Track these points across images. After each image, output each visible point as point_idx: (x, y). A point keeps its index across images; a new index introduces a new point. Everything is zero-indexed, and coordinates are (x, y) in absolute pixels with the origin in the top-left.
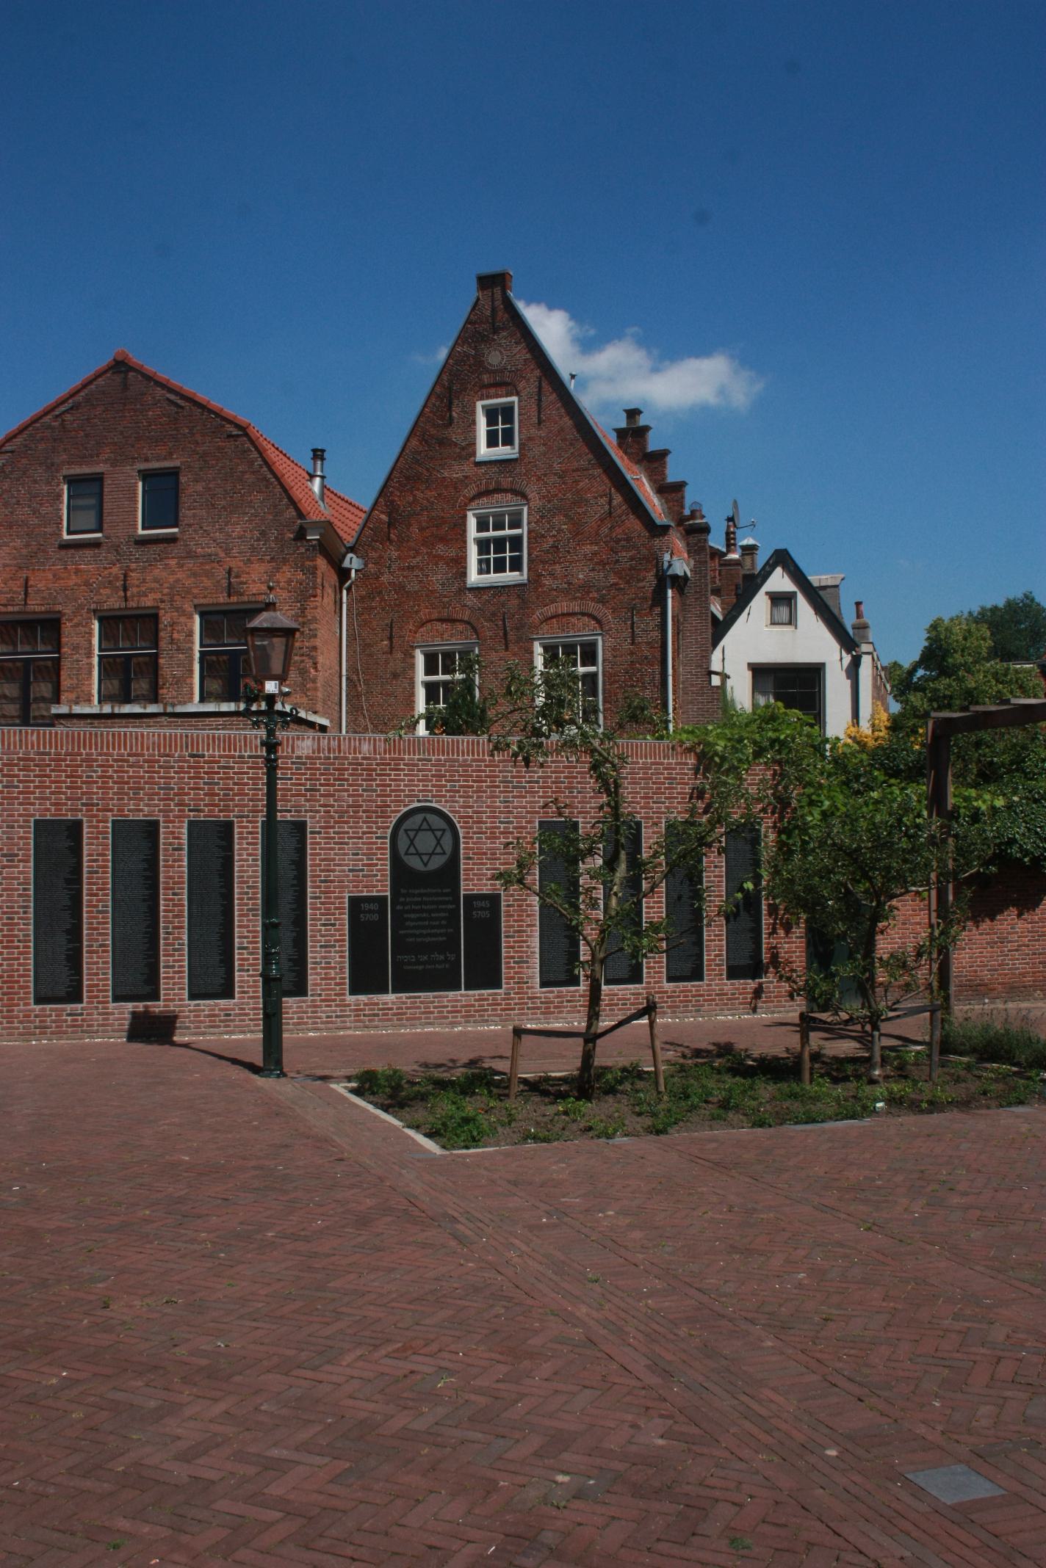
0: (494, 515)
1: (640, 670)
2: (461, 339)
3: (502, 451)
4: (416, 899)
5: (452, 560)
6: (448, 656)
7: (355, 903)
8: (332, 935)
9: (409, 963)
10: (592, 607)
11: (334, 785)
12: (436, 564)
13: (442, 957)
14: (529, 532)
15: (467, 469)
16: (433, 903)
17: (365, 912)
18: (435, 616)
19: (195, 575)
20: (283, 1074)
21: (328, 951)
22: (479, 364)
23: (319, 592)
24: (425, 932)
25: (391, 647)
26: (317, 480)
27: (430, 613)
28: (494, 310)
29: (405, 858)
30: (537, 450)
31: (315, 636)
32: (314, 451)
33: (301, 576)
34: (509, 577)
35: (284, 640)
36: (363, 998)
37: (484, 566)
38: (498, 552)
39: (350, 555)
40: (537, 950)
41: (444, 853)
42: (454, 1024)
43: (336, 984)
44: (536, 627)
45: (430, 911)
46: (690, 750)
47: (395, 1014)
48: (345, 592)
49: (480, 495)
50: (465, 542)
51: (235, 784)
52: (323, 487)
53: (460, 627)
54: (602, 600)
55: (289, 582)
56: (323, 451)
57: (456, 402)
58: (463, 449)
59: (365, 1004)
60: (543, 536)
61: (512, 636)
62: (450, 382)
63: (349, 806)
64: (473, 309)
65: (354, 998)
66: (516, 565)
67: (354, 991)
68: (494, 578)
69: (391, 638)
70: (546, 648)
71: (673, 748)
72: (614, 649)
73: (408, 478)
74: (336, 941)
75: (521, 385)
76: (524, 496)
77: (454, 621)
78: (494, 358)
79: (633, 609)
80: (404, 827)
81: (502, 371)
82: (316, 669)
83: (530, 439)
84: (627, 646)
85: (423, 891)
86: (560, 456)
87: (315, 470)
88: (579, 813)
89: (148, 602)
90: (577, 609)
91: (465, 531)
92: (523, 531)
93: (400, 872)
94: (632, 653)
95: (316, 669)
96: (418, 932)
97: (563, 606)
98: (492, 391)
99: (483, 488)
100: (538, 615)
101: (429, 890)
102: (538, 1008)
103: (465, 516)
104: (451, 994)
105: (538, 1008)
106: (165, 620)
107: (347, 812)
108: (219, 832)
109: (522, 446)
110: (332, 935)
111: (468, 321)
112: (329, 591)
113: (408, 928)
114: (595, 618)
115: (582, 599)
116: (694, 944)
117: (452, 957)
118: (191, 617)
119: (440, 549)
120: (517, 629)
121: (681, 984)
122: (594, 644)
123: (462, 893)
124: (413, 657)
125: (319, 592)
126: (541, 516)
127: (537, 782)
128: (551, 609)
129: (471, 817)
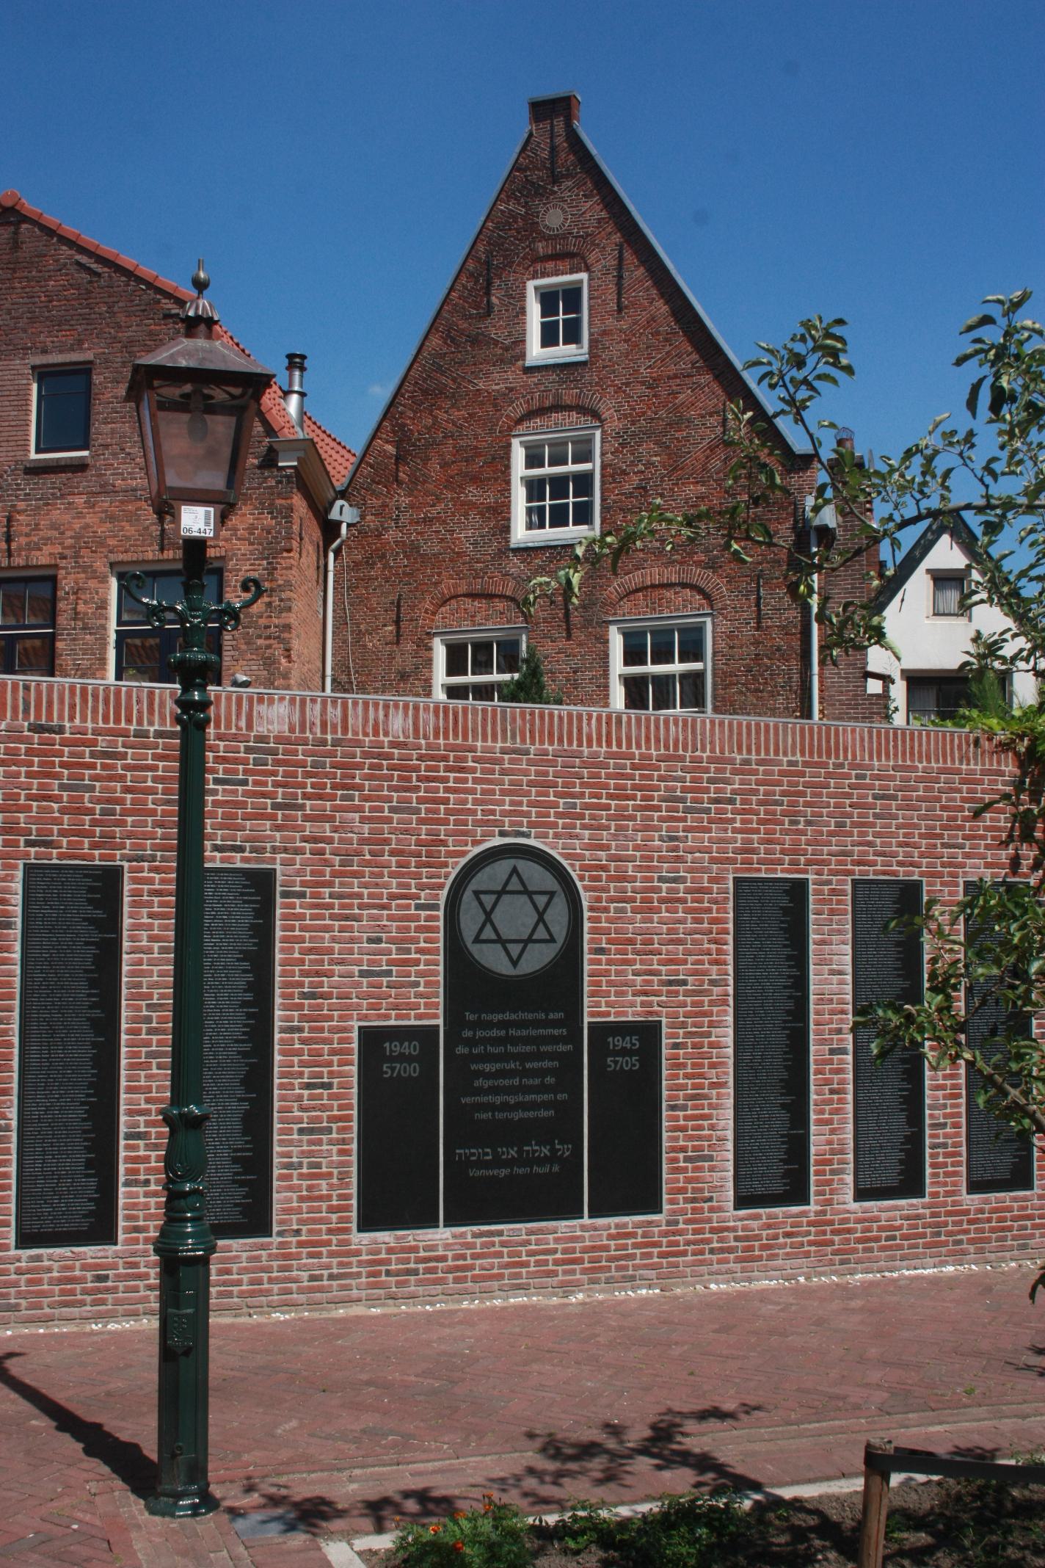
0: (552, 444)
1: (768, 668)
2: (506, 193)
3: (564, 352)
4: (495, 1033)
5: (489, 508)
6: (482, 648)
7: (372, 1039)
8: (323, 1108)
11: (333, 798)
12: (466, 515)
13: (546, 1151)
14: (603, 467)
15: (513, 376)
17: (392, 1059)
18: (463, 589)
19: (112, 518)
20: (208, 1503)
21: (315, 1144)
22: (531, 229)
23: (295, 544)
24: (512, 1100)
25: (398, 635)
26: (294, 399)
27: (455, 586)
28: (553, 150)
29: (475, 949)
30: (616, 349)
32: (291, 357)
33: (268, 521)
34: (571, 532)
35: (232, 420)
36: (386, 1237)
37: (535, 518)
38: (556, 499)
39: (339, 503)
40: (730, 1134)
41: (552, 940)
42: (567, 1287)
43: (332, 1210)
44: (613, 605)
45: (523, 1058)
46: (1005, 747)
47: (450, 1270)
48: (331, 556)
49: (530, 415)
50: (508, 483)
51: (127, 790)
52: (302, 412)
53: (500, 605)
54: (712, 565)
55: (251, 529)
56: (303, 357)
58: (506, 349)
60: (624, 473)
61: (576, 618)
62: (489, 253)
63: (362, 841)
64: (524, 149)
65: (367, 1237)
66: (583, 516)
67: (366, 1224)
68: (550, 534)
69: (397, 622)
70: (627, 635)
71: (977, 742)
72: (730, 636)
73: (425, 392)
74: (332, 1119)
75: (591, 258)
76: (596, 415)
77: (490, 596)
78: (554, 219)
79: (759, 577)
80: (474, 885)
81: (564, 237)
82: (289, 657)
83: (604, 333)
84: (749, 632)
85: (508, 1016)
87: (291, 384)
88: (809, 863)
89: (41, 558)
90: (674, 579)
91: (508, 467)
92: (595, 466)
93: (465, 979)
94: (757, 643)
95: (289, 657)
96: (498, 1100)
97: (655, 574)
99: (535, 404)
101: (522, 1016)
102: (730, 1250)
103: (508, 446)
104: (563, 1225)
105: (730, 1250)
106: (66, 584)
107: (359, 853)
108: (91, 890)
109: (593, 343)
110: (323, 1108)
111: (516, 167)
113: (480, 1092)
114: (700, 591)
115: (681, 563)
117: (565, 1150)
118: (104, 580)
119: (472, 493)
121: (992, 1196)
122: (700, 629)
123: (586, 1020)
124: (431, 649)
125: (295, 544)
126: (622, 442)
127: (731, 801)
128: (636, 579)
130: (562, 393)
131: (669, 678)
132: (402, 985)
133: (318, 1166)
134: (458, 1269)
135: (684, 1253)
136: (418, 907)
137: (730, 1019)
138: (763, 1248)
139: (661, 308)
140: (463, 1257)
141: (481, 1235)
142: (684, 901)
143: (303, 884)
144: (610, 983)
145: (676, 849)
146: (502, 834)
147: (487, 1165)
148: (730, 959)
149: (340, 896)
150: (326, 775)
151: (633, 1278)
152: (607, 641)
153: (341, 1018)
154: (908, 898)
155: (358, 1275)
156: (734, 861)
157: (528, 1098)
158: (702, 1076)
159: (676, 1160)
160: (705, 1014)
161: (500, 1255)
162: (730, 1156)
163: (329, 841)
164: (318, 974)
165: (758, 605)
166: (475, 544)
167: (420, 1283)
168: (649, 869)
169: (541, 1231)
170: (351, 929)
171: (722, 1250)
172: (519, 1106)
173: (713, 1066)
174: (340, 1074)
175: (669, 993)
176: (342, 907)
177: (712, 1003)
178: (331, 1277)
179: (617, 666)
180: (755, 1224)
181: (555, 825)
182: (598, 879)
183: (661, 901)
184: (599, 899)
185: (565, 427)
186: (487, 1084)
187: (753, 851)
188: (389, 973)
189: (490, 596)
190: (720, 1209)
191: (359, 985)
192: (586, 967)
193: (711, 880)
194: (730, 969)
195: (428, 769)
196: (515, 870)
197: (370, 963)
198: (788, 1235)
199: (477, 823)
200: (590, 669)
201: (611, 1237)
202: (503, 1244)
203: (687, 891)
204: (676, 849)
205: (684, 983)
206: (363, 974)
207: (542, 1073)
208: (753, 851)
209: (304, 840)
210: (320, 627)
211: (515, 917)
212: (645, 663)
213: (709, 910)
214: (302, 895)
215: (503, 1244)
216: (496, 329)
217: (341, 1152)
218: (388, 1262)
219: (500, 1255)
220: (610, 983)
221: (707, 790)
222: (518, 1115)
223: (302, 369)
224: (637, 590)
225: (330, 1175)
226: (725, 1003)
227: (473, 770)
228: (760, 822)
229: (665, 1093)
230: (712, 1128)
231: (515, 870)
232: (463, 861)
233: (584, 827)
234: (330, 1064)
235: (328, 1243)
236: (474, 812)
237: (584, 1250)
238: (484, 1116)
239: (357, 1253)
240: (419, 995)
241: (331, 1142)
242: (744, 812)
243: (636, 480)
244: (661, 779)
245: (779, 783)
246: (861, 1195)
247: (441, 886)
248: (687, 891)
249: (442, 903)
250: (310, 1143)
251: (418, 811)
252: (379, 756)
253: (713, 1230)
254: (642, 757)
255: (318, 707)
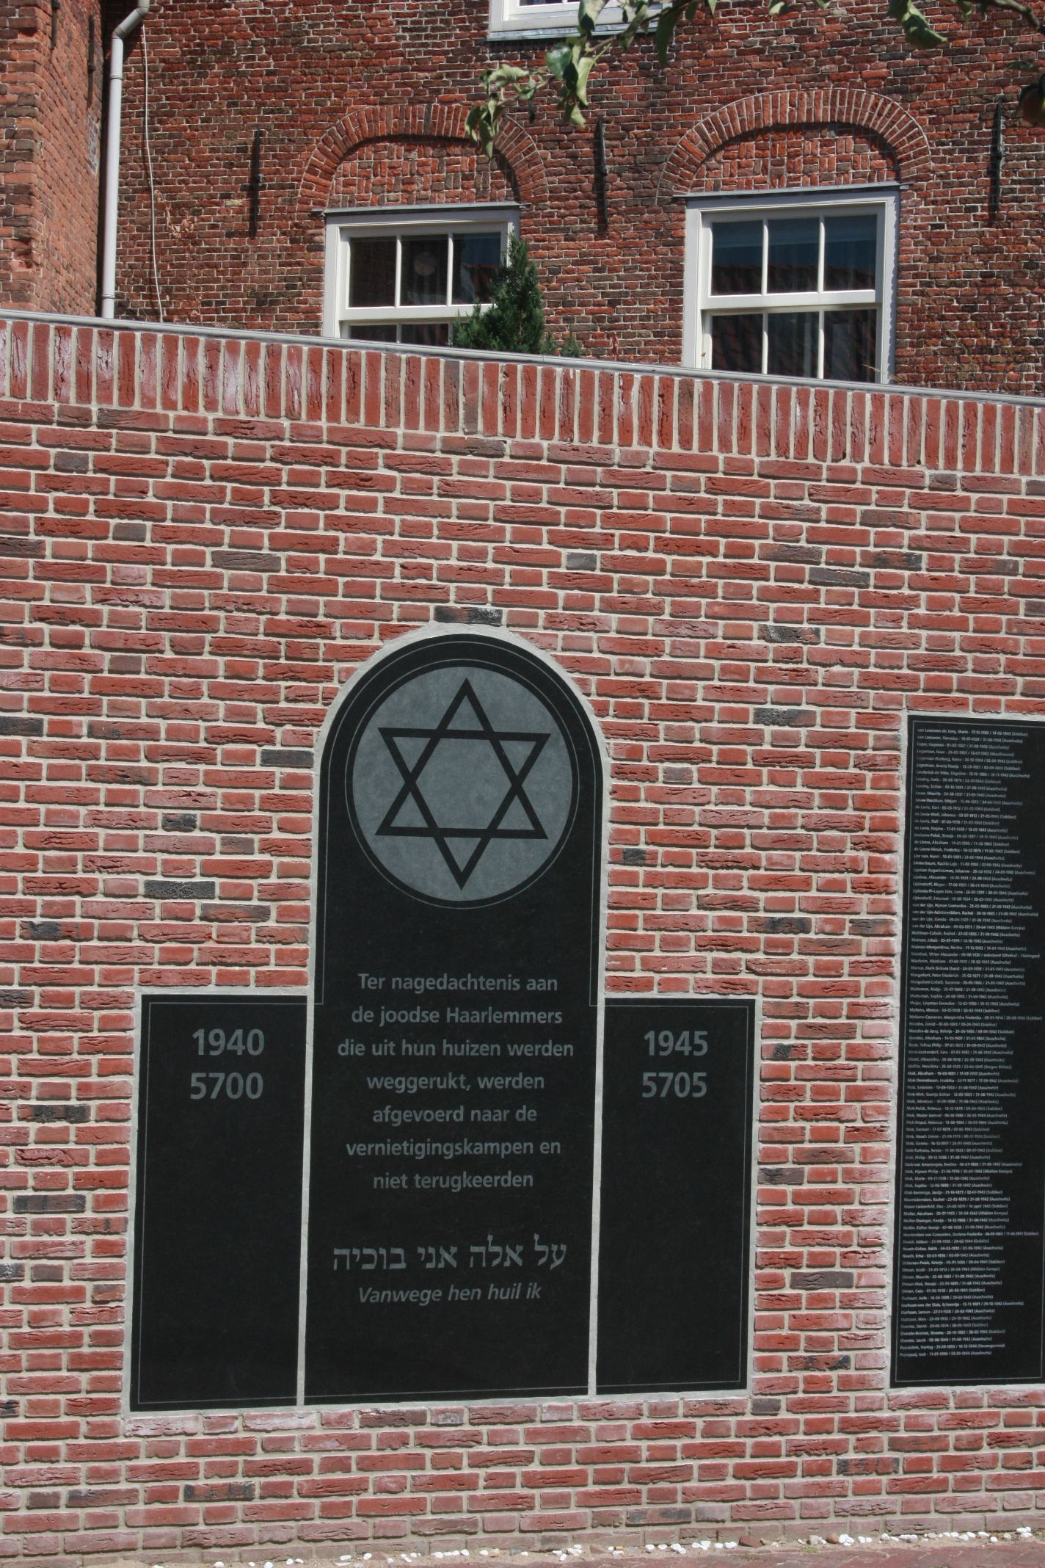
1: (1008, 303)
4: (417, 1016)
6: (425, 248)
7: (171, 1024)
8: (67, 1159)
9: (383, 1279)
10: (868, 106)
11: (98, 532)
13: (514, 1256)
16: (483, 1033)
17: (209, 1064)
18: (389, 124)
23: (42, 18)
24: (449, 1151)
25: (254, 217)
27: (373, 117)
29: (382, 847)
31: (29, 155)
36: (187, 1421)
40: (887, 1233)
41: (538, 833)
43: (79, 1364)
44: (694, 165)
48: (118, 46)
54: (903, 87)
59: (196, 1449)
61: (618, 190)
63: (159, 623)
69: (252, 190)
70: (720, 230)
72: (934, 235)
74: (86, 1182)
80: (383, 717)
84: (972, 228)
90: (823, 113)
94: (987, 250)
95: (27, 254)
96: (421, 1150)
97: (782, 101)
100: (695, 135)
101: (474, 982)
102: (882, 1467)
105: (882, 1467)
107: (151, 647)
110: (67, 1159)
112: (73, 28)
114: (876, 140)
115: (838, 81)
117: (553, 1255)
120: (636, 169)
122: (871, 220)
123: (603, 994)
124: (320, 248)
125: (42, 18)
127: (910, 562)
128: (744, 111)
129: (647, 691)
131: (805, 319)
132: (231, 916)
133: (55, 1275)
134: (331, 1488)
135: (788, 1471)
136: (269, 759)
137: (893, 1002)
138: (948, 1464)
140: (343, 1465)
141: (380, 1421)
142: (806, 761)
143: (36, 705)
144: (653, 923)
145: (794, 656)
146: (443, 616)
147: (397, 1281)
148: (897, 881)
149: (112, 733)
150: (88, 486)
151: (683, 1517)
152: (680, 241)
153: (108, 979)
155: (131, 1496)
156: (911, 684)
157: (481, 1148)
158: (832, 1114)
159: (776, 1282)
160: (842, 991)
161: (417, 1462)
162: (887, 1277)
163: (91, 620)
164: (62, 888)
165: (993, 172)
166: (415, 29)
167: (254, 1516)
168: (739, 695)
169: (501, 1417)
170: (132, 801)
171: (864, 1467)
172: (463, 1163)
173: (856, 1095)
174: (104, 1093)
175: (771, 947)
176: (115, 754)
177: (857, 969)
178: (75, 1500)
179: (700, 292)
180: (932, 1416)
181: (550, 601)
182: (635, 712)
184: (635, 754)
186: (400, 1118)
187: (953, 665)
188: (207, 891)
189: (444, 142)
190: (862, 1384)
191: (145, 912)
192: (606, 890)
193: (864, 722)
194: (897, 901)
195: (296, 479)
196: (466, 690)
197: (169, 868)
198: (998, 1441)
199: (392, 593)
200: (643, 298)
201: (641, 1433)
202: (424, 1441)
203: (815, 742)
204: (794, 656)
205: (803, 926)
206: (154, 890)
207: (511, 1099)
208: (953, 665)
209: (40, 616)
210: (92, 199)
211: (464, 784)
212: (754, 288)
213: (857, 782)
214: (33, 728)
215: (424, 1441)
217: (101, 1249)
218: (190, 1471)
219: (417, 1462)
220: (653, 923)
221: (862, 539)
222: (460, 1183)
224: (746, 136)
225: (78, 1294)
226: (885, 970)
227: (388, 485)
228: (968, 606)
229: (757, 1147)
230: (851, 1219)
231: (466, 690)
232: (362, 668)
233: (609, 606)
234: (83, 1070)
235: (71, 1431)
236: (386, 570)
237: (587, 1458)
238: (392, 1182)
239: (129, 1453)
240: (269, 937)
241: (81, 1228)
242: (935, 584)
244: (768, 513)
245: (1010, 529)
247: (316, 719)
248: (815, 742)
249: (317, 751)
250: (39, 1228)
251: (271, 565)
252: (196, 450)
253: (847, 1427)
254: (732, 467)
255: (72, 345)
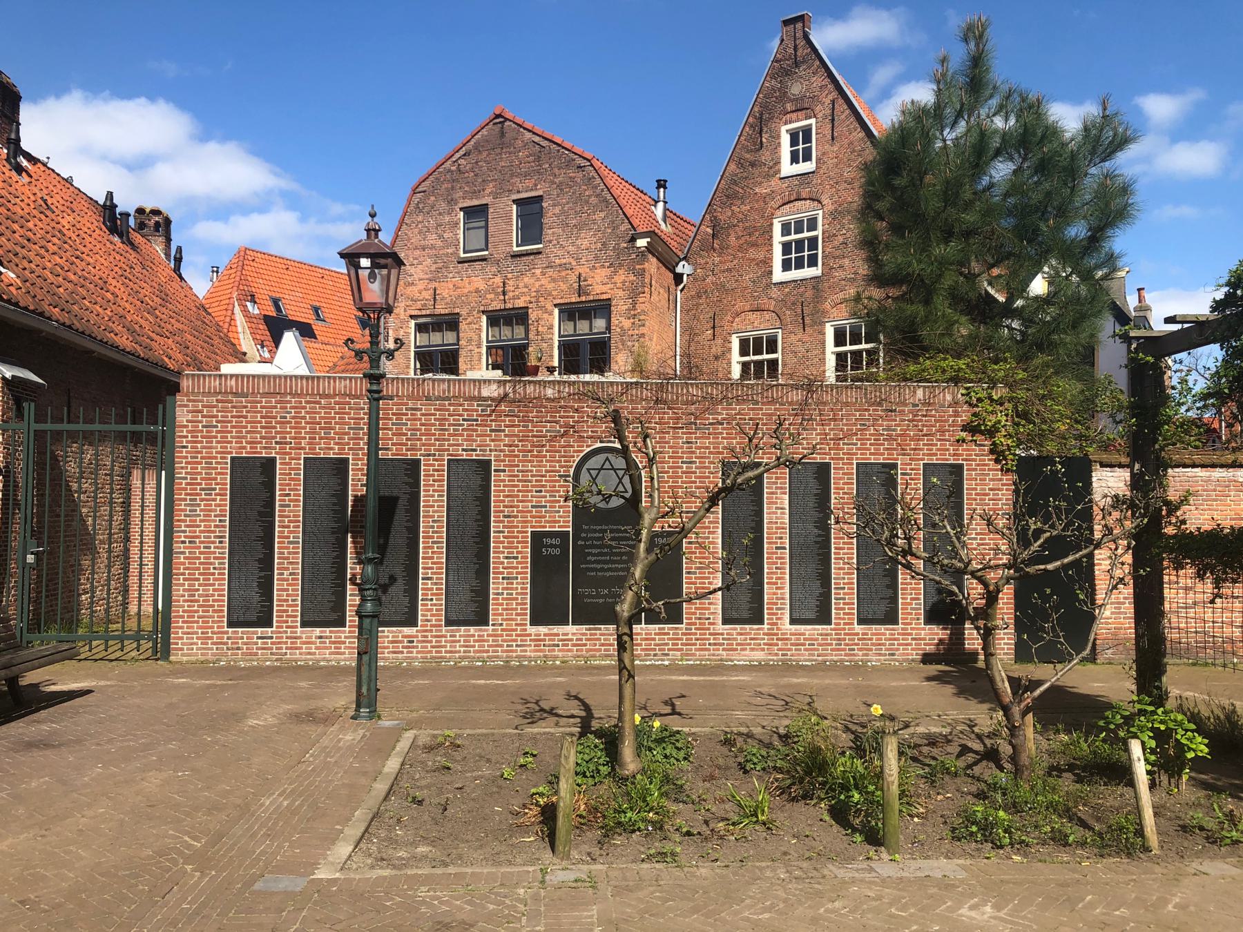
2: (772, 75)
3: (808, 167)
4: (597, 535)
6: (758, 341)
7: (538, 538)
9: (590, 596)
17: (547, 546)
19: (554, 280)
21: (511, 583)
22: (783, 95)
24: (606, 567)
26: (661, 205)
32: (658, 181)
33: (632, 278)
36: (543, 630)
55: (624, 282)
57: (765, 129)
60: (835, 235)
62: (761, 114)
66: (813, 262)
67: (535, 621)
68: (795, 274)
73: (727, 197)
80: (586, 466)
81: (802, 98)
86: (850, 166)
89: (520, 303)
92: (819, 232)
96: (599, 566)
98: (794, 116)
99: (787, 199)
103: (772, 224)
106: (533, 316)
108: (406, 469)
109: (818, 160)
116: (888, 586)
118: (551, 314)
119: (752, 253)
130: (801, 190)
139: (862, 134)
147: (593, 597)
154: (887, 474)
172: (602, 570)
183: (683, 472)
185: (803, 211)
216: (765, 156)
222: (608, 574)
223: (665, 188)
243: (841, 239)
246: (793, 621)
